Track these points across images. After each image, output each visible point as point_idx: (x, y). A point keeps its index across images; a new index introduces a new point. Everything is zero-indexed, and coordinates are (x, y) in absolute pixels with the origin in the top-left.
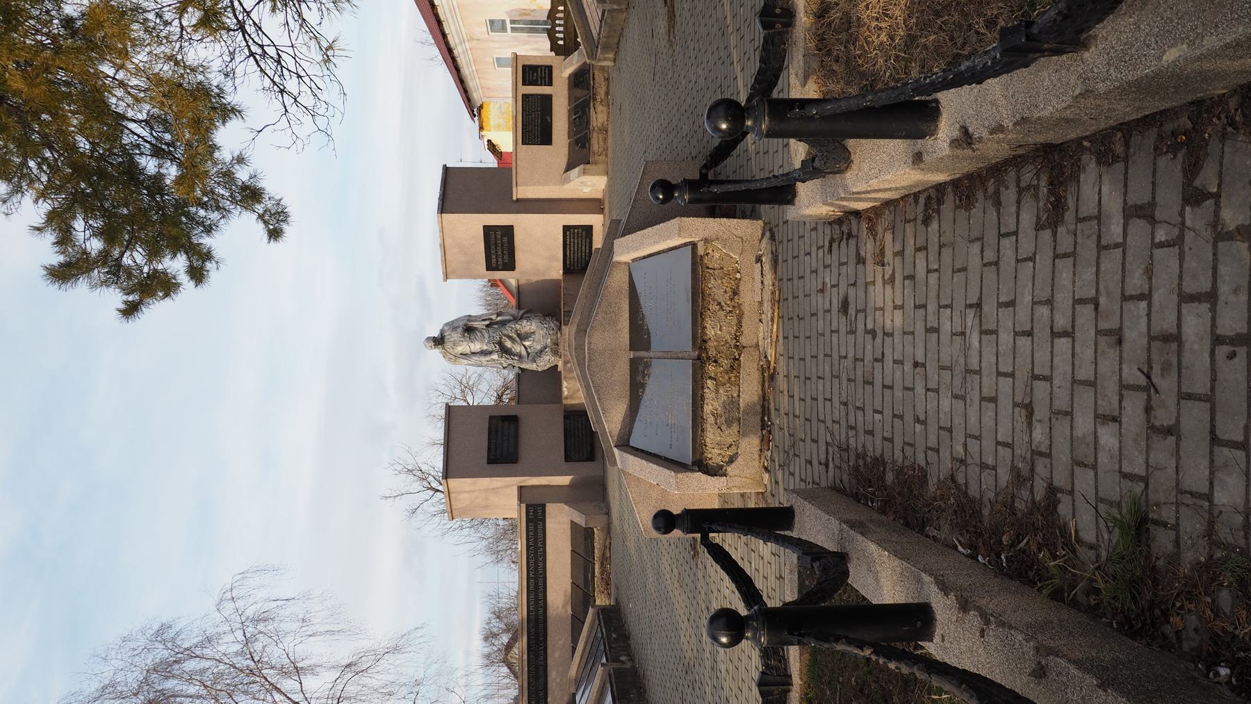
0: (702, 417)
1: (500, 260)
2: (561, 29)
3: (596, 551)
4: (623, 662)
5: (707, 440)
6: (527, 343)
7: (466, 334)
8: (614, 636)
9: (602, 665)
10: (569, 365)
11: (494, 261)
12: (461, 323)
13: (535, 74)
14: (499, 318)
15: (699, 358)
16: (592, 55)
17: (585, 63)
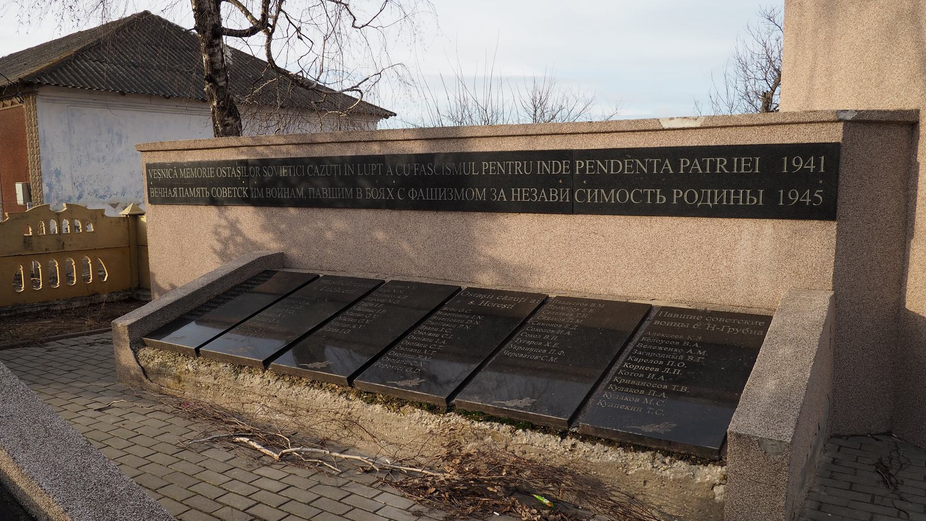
3: (612, 456)
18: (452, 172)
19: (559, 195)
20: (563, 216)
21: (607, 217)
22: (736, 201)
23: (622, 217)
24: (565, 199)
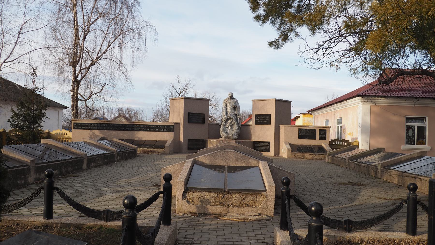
0: (204, 191)
1: (259, 120)
2: (339, 144)
3: (156, 149)
4: (117, 158)
5: (196, 193)
6: (229, 128)
8: (127, 155)
9: (117, 150)
10: (221, 142)
11: (258, 117)
12: (237, 105)
13: (323, 134)
14: (238, 118)
15: (225, 191)
16: (330, 154)
17: (327, 152)
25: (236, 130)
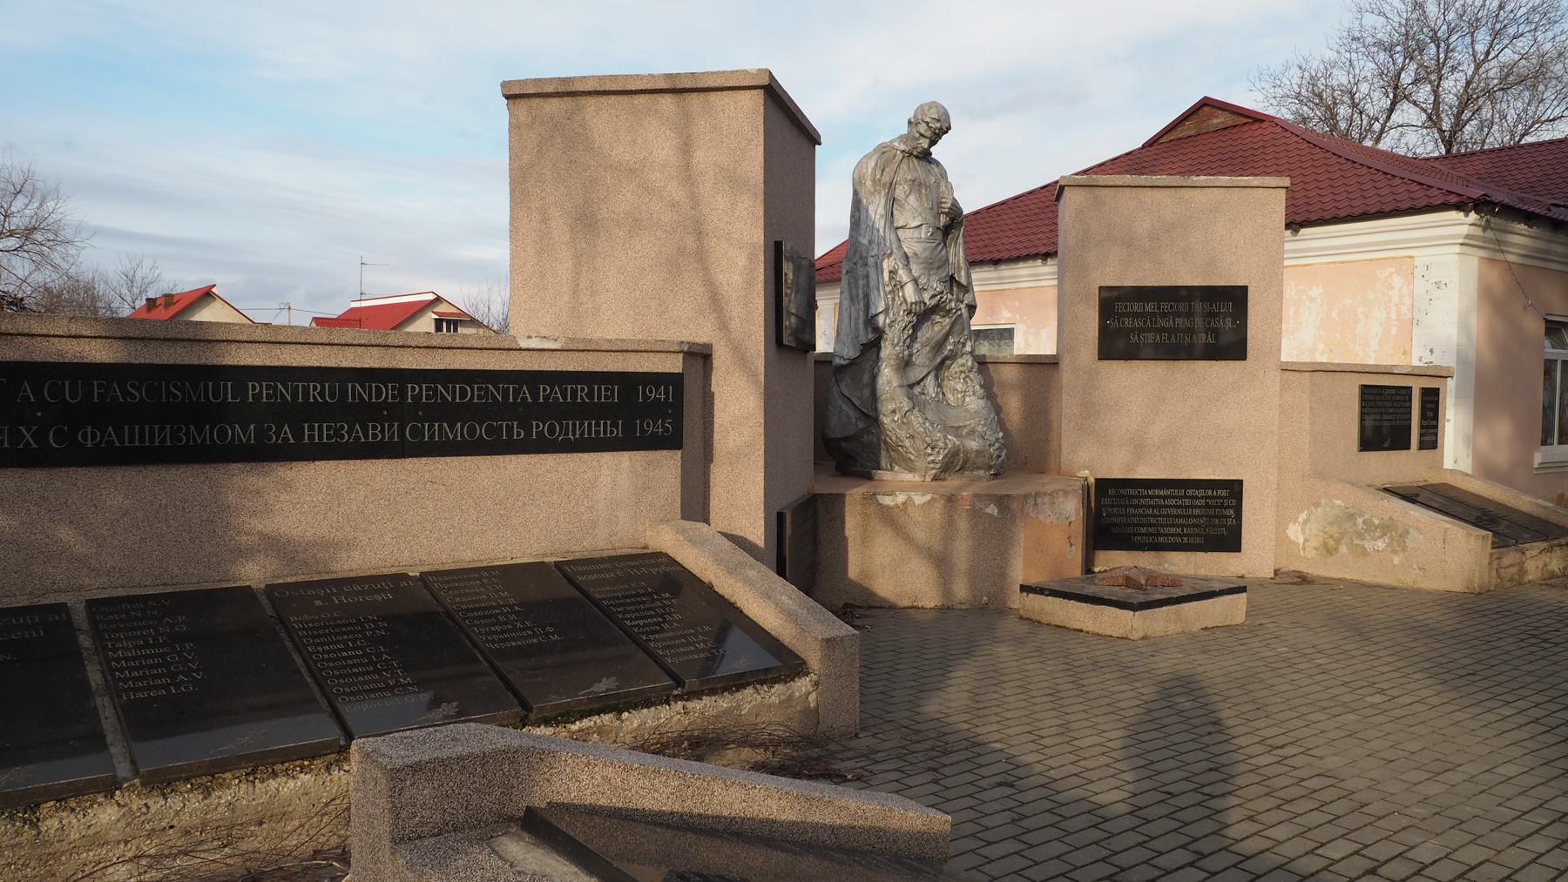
3: (724, 702)
7: (943, 220)
18: (184, 398)
19: (382, 431)
20: (386, 461)
21: (448, 459)
22: (598, 432)
23: (469, 458)
24: (392, 437)
25: (982, 402)
